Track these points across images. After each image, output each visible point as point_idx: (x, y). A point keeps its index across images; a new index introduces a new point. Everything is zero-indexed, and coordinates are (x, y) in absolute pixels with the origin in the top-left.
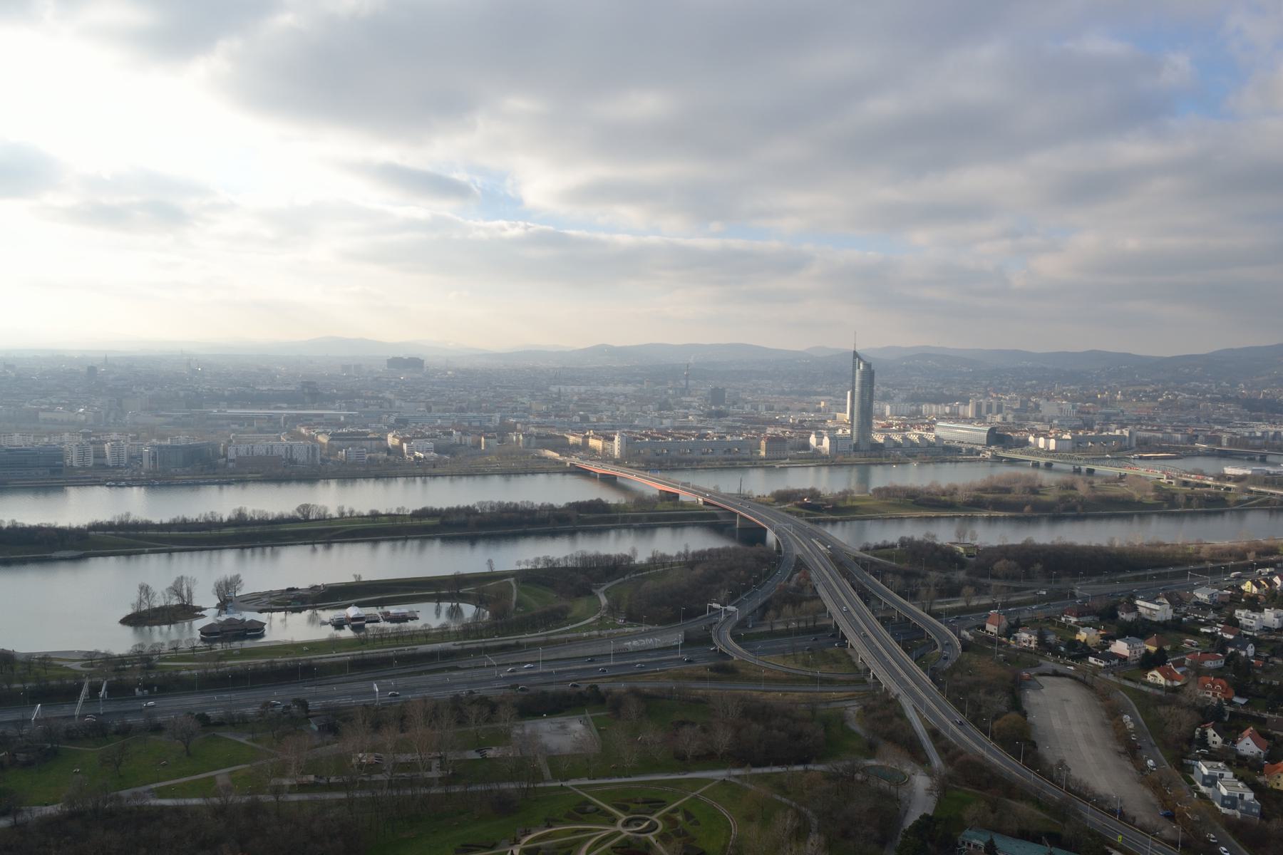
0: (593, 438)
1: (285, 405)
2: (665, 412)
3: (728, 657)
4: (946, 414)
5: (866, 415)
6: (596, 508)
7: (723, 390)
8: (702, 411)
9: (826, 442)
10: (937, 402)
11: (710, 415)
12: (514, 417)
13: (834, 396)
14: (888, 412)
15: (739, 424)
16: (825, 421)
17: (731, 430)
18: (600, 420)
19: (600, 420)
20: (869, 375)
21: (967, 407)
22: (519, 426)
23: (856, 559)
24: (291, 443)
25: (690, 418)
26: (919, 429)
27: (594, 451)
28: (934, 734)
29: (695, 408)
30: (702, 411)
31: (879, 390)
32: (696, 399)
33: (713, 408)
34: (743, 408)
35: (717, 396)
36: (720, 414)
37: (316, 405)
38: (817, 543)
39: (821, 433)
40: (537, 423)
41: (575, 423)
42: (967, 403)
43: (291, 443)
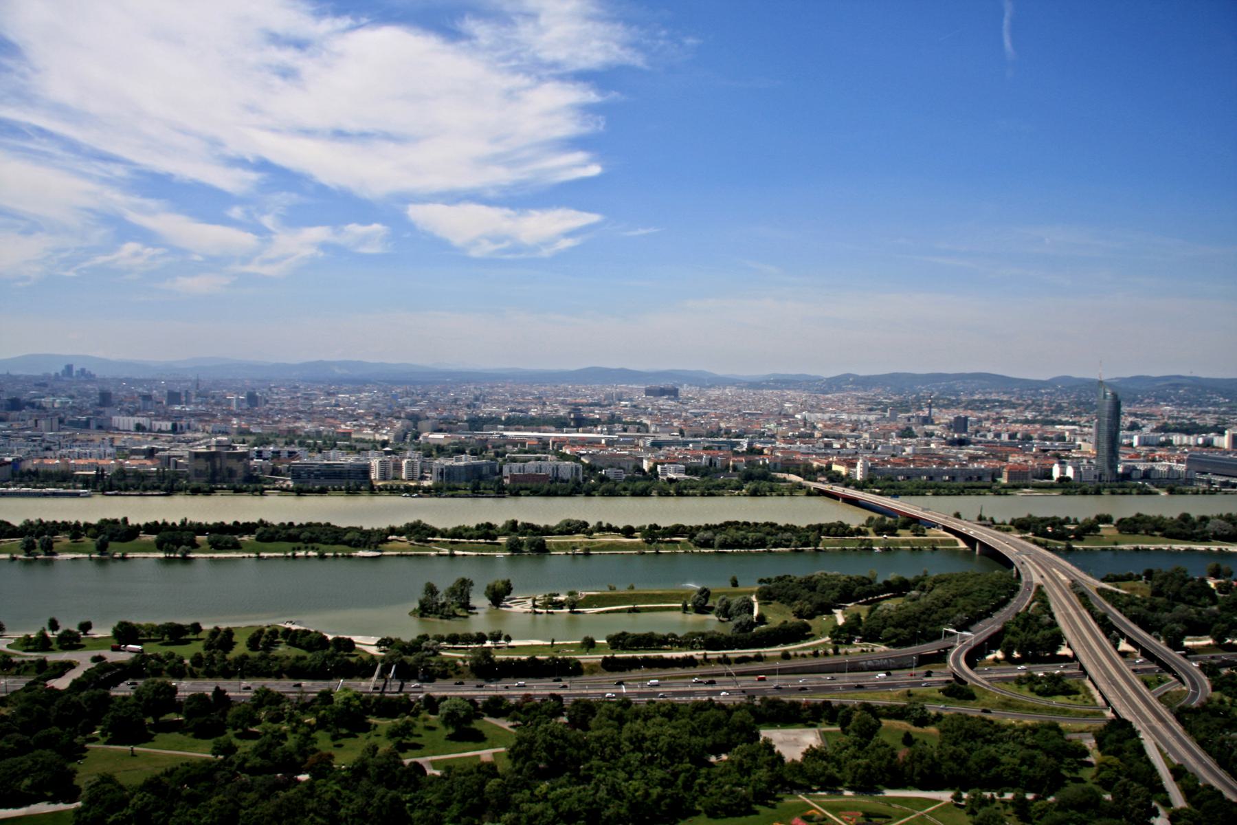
0: (836, 463)
1: (553, 429)
2: (908, 439)
3: (965, 683)
4: (1198, 445)
5: (1113, 445)
6: (840, 530)
7: (966, 419)
8: (945, 439)
9: (1070, 472)
10: (1188, 432)
11: (953, 443)
12: (761, 443)
13: (1080, 426)
14: (1136, 443)
15: (980, 452)
16: (1069, 450)
17: (973, 458)
18: (843, 446)
19: (843, 446)
20: (1117, 405)
21: (1221, 438)
22: (766, 451)
23: (1100, 591)
24: (557, 463)
25: (933, 446)
26: (1169, 460)
27: (838, 474)
28: (1179, 773)
29: (937, 436)
30: (945, 439)
31: (1126, 421)
32: (938, 427)
33: (956, 436)
34: (985, 436)
35: (960, 424)
36: (962, 443)
37: (580, 429)
38: (1057, 572)
39: (1064, 463)
40: (783, 448)
41: (820, 449)
42: (1221, 433)
43: (557, 463)
